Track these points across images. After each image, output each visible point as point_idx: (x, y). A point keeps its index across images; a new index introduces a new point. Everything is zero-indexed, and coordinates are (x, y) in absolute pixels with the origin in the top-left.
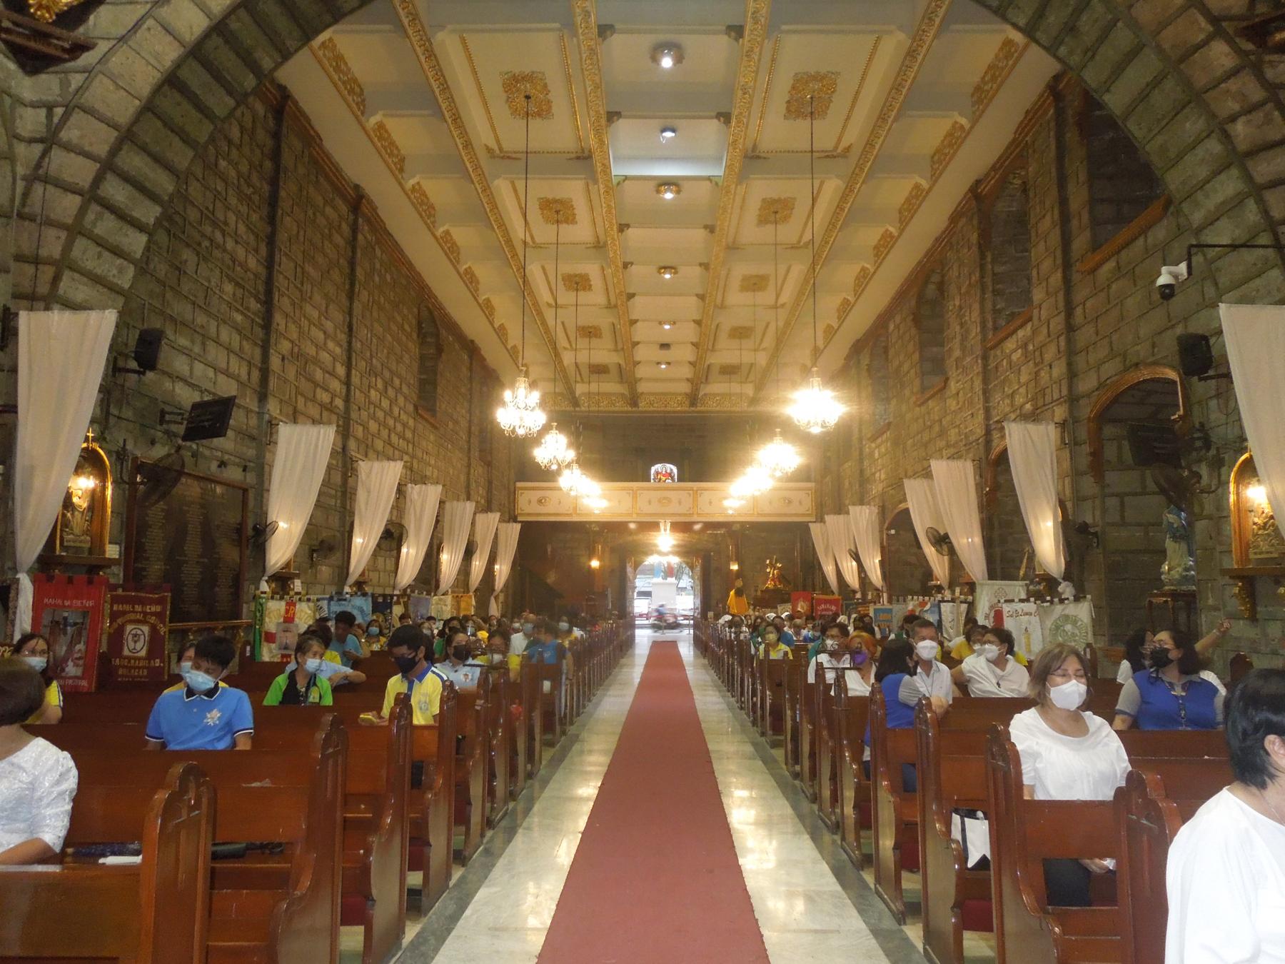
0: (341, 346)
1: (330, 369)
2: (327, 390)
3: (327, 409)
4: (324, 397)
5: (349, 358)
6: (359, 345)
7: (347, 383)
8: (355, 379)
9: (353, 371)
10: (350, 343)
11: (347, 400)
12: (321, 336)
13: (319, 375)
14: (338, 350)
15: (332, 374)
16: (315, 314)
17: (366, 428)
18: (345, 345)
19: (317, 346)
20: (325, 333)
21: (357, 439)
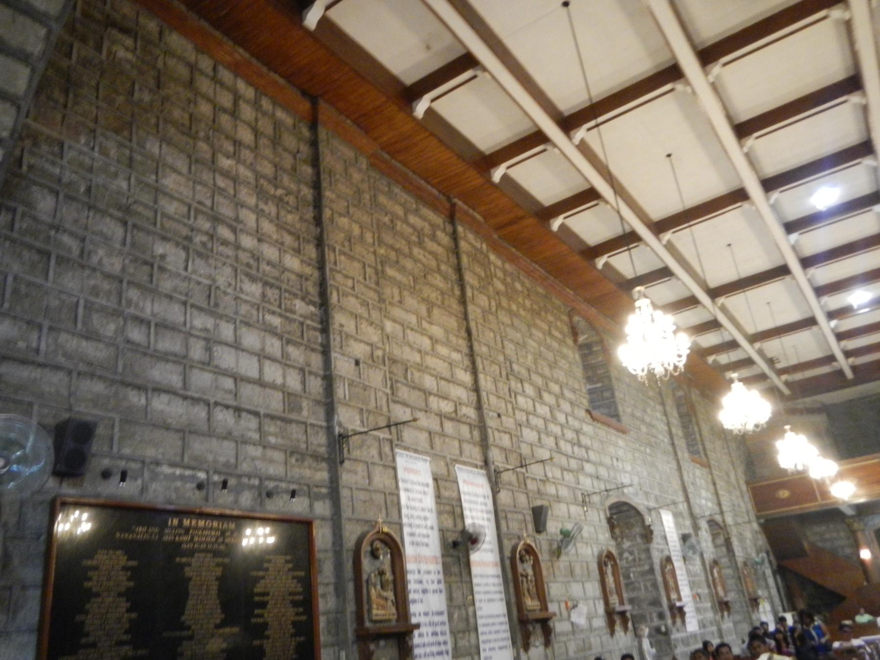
0: (459, 351)
1: (446, 374)
2: (447, 399)
3: (452, 419)
4: (446, 407)
5: (473, 363)
6: (484, 349)
7: (476, 388)
8: (485, 383)
9: (481, 376)
10: (471, 348)
11: (479, 407)
12: (426, 343)
13: (429, 382)
14: (456, 356)
15: (452, 380)
16: (413, 319)
17: (516, 437)
18: (465, 350)
19: (419, 351)
20: (431, 338)
21: (503, 449)
